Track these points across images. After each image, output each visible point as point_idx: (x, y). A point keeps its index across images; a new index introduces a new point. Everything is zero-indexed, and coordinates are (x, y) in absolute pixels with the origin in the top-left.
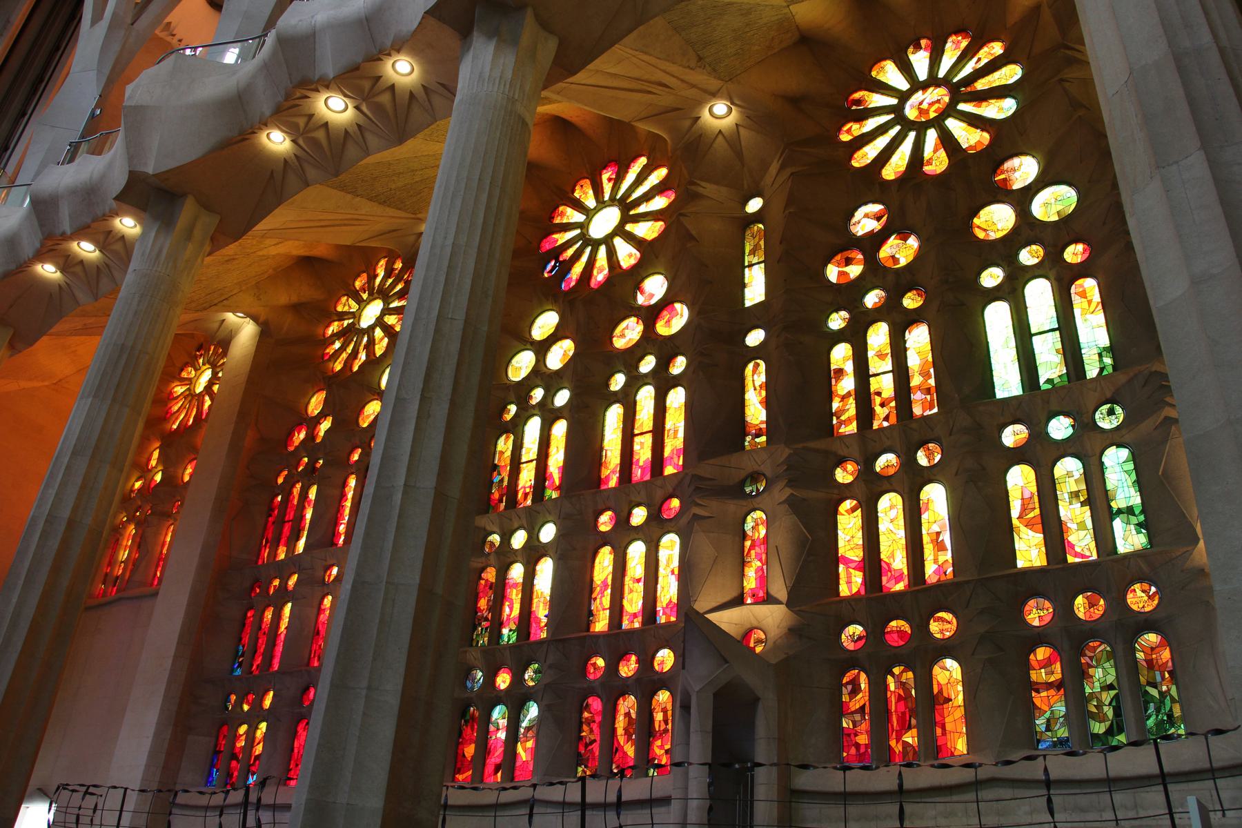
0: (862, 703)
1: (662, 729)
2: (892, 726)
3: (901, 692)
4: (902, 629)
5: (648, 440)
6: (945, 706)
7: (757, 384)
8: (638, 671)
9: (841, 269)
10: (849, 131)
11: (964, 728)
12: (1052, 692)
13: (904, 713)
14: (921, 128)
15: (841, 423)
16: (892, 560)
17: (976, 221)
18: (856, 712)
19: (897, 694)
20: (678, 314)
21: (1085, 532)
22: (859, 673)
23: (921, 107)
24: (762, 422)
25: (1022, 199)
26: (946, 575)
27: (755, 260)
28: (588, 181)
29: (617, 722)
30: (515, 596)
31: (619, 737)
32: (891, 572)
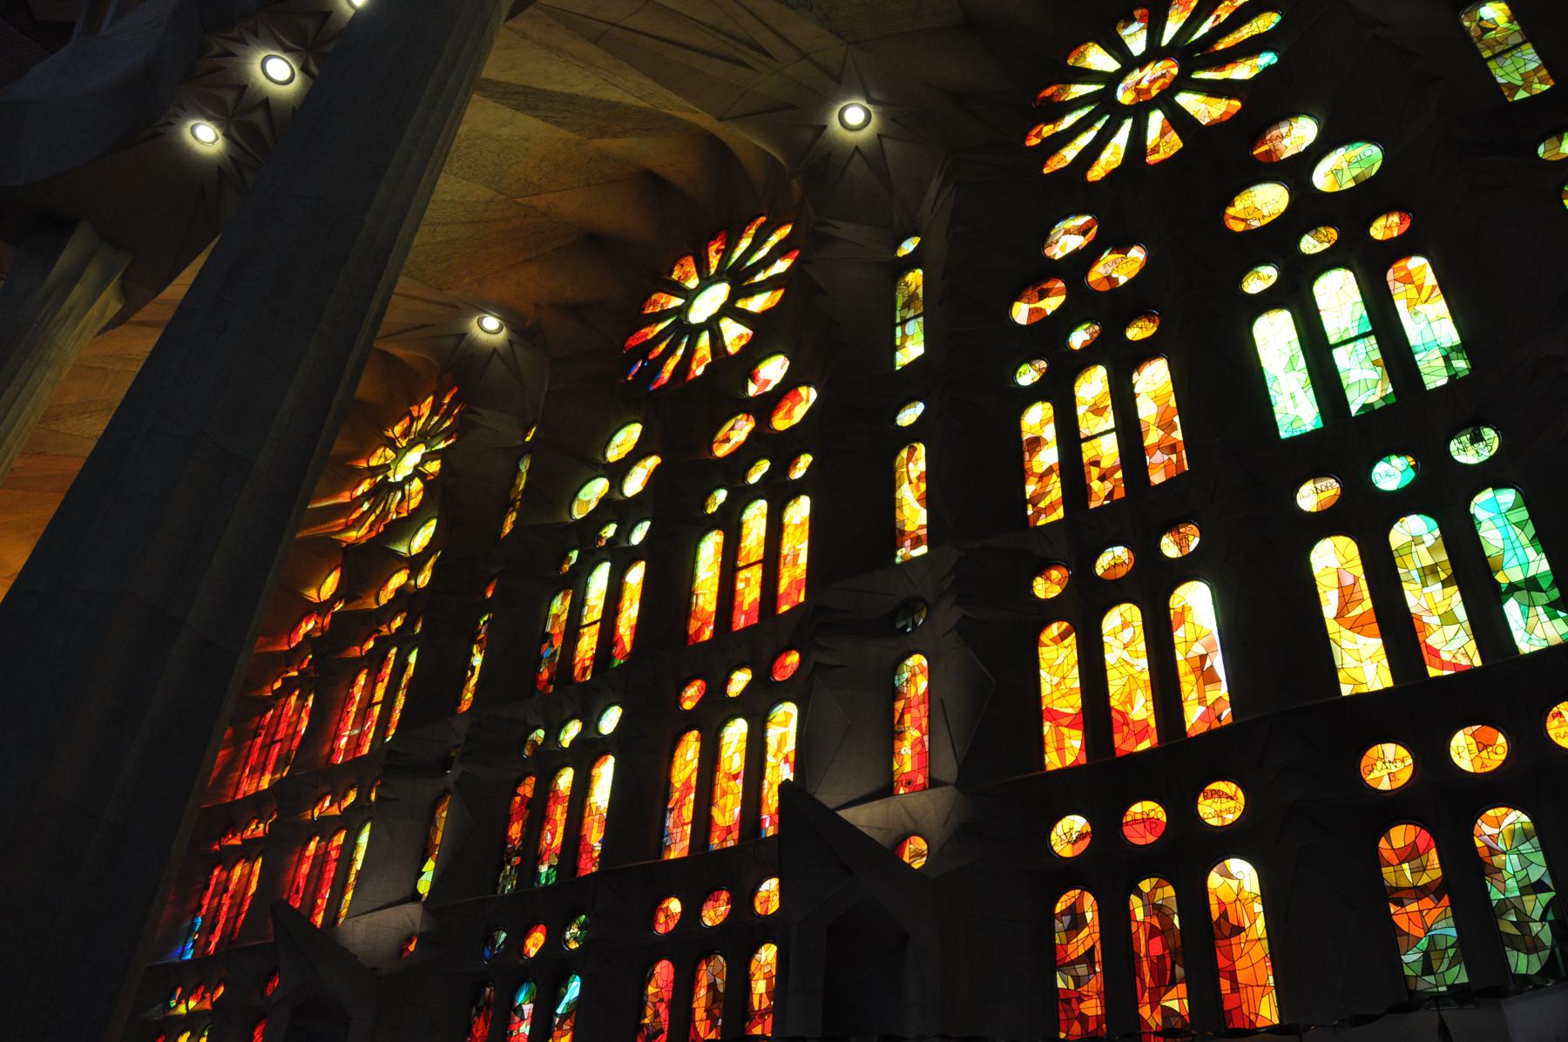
0: (1089, 945)
1: (763, 1006)
2: (1143, 980)
3: (1155, 922)
4: (1151, 816)
5: (756, 574)
6: (1234, 940)
7: (914, 476)
8: (730, 916)
9: (1033, 306)
10: (1037, 135)
11: (1271, 978)
12: (1427, 902)
13: (1161, 958)
14: (1139, 112)
15: (1039, 512)
16: (1129, 706)
17: (1231, 211)
18: (1079, 960)
19: (1149, 926)
20: (802, 400)
21: (1452, 629)
22: (1081, 896)
23: (1139, 87)
24: (921, 527)
25: (1296, 171)
26: (1220, 721)
27: (911, 314)
28: (691, 259)
29: (695, 999)
30: (559, 814)
31: (697, 1024)
32: (1128, 725)
